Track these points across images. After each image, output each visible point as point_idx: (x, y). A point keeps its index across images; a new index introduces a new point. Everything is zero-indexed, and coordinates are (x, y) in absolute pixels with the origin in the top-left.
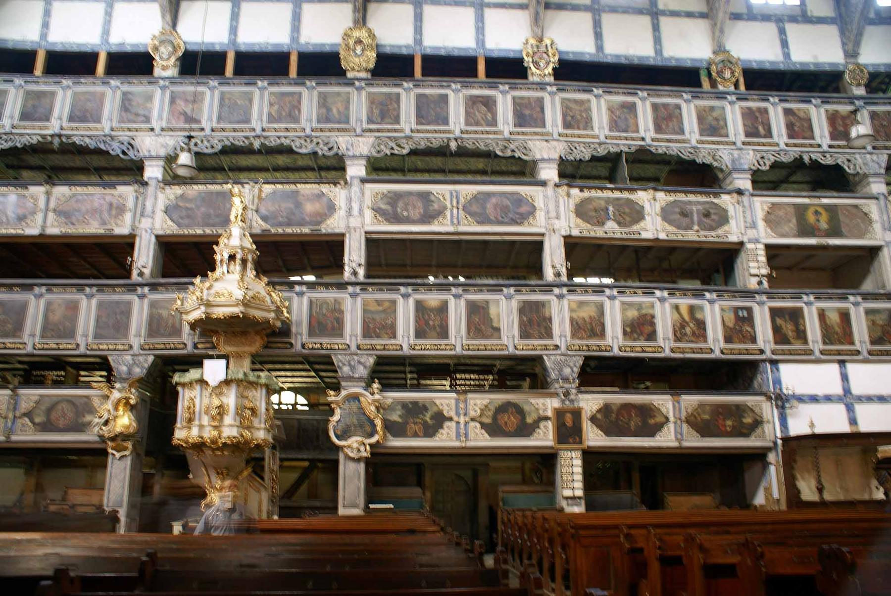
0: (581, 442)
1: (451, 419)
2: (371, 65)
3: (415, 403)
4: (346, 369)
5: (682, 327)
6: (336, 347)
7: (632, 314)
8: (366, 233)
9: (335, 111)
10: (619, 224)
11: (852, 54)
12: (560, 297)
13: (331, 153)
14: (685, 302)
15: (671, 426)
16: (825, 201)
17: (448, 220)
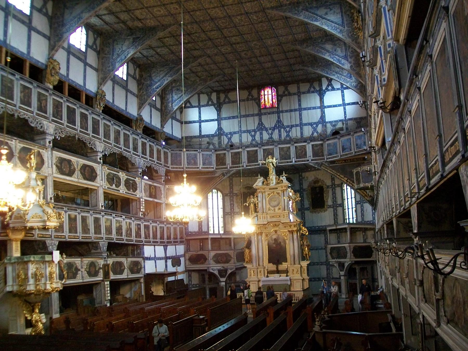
0: (109, 278)
1: (79, 270)
2: (56, 83)
3: (70, 263)
4: (51, 247)
5: (128, 231)
6: (47, 236)
7: (118, 225)
8: (54, 177)
9: (43, 105)
10: (116, 186)
11: (162, 126)
12: (103, 216)
13: (41, 130)
14: (128, 221)
15: (126, 270)
16: (155, 184)
17: (76, 176)
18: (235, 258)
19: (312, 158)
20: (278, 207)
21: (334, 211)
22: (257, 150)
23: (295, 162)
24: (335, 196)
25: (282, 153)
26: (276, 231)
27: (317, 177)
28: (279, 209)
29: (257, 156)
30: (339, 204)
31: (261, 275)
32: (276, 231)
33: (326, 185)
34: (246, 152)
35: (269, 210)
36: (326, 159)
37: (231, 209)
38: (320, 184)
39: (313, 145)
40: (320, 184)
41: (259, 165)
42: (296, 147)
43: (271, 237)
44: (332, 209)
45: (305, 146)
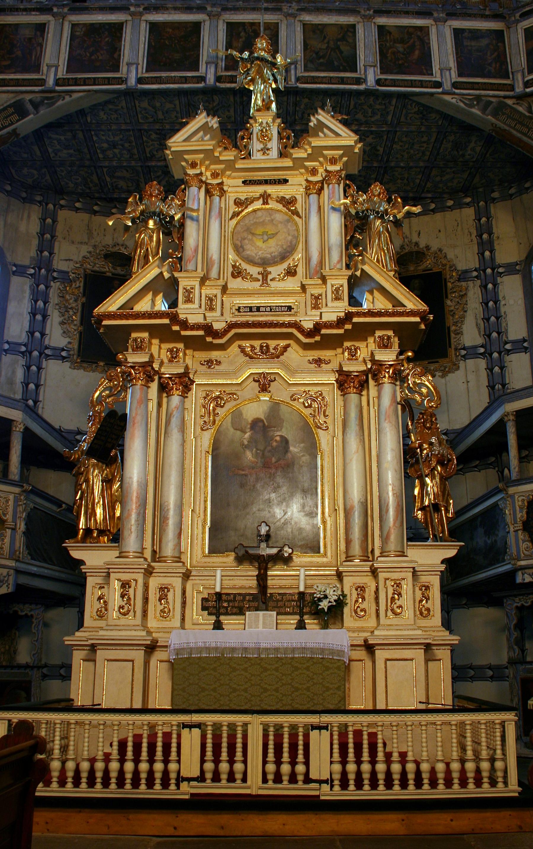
18: (22, 526)
19: (455, 78)
20: (285, 265)
21: (490, 369)
22: (197, 26)
23: (378, 82)
24: (497, 309)
25: (316, 44)
26: (264, 383)
27: (415, 239)
28: (291, 272)
29: (197, 46)
30: (513, 342)
31: (164, 614)
32: (264, 383)
33: (453, 268)
34: (144, 29)
35: (237, 273)
36: (519, 88)
37: (31, 333)
38: (428, 263)
39: (457, 33)
40: (428, 263)
41: (202, 79)
42: (381, 29)
43: (237, 415)
44: (482, 363)
45: (424, 31)
